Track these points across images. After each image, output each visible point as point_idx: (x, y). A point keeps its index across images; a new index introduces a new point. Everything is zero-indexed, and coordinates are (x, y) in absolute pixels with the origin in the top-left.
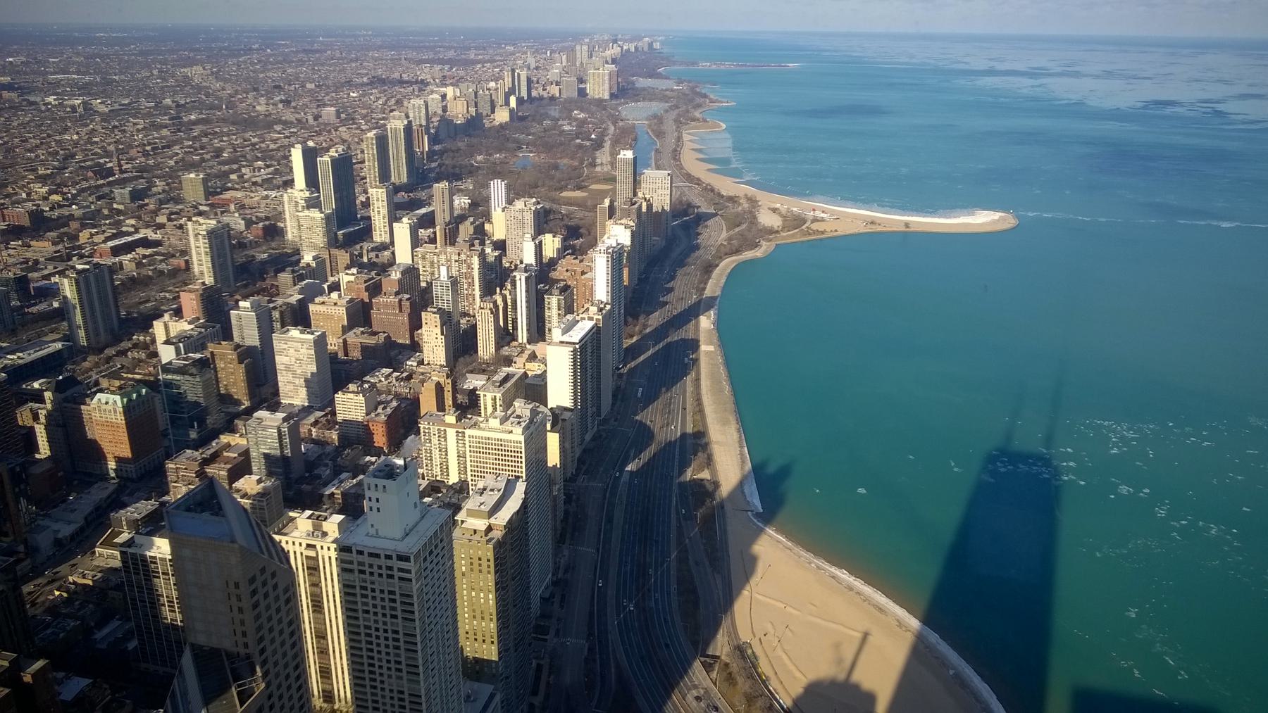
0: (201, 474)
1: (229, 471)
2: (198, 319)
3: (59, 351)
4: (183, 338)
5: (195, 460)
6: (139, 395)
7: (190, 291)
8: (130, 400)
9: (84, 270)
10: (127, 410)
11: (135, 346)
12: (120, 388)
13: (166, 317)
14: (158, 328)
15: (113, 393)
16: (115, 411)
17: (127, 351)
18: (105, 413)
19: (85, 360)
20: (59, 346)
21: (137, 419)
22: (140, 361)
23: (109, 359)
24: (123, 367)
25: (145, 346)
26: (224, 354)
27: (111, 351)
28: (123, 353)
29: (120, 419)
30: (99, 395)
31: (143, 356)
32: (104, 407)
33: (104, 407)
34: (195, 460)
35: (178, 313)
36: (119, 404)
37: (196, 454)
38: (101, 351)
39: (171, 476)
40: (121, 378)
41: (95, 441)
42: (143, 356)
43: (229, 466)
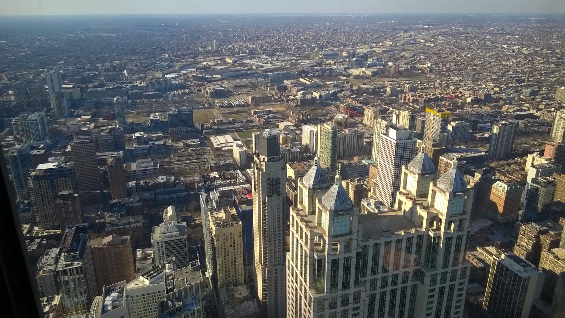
0: (537, 237)
1: (551, 241)
2: (551, 159)
3: (483, 156)
4: (541, 167)
5: (536, 229)
6: (516, 188)
7: (551, 145)
8: (511, 189)
9: (505, 124)
10: (508, 192)
11: (516, 163)
12: (509, 182)
13: (535, 154)
14: (530, 158)
15: (505, 183)
16: (503, 191)
17: (511, 164)
18: (499, 190)
19: (492, 162)
20: (483, 153)
21: (512, 197)
22: (516, 170)
23: (502, 166)
24: (507, 171)
25: (520, 164)
26: (560, 181)
27: (504, 162)
28: (509, 165)
29: (504, 195)
30: (498, 182)
31: (518, 169)
32: (499, 188)
33: (499, 188)
34: (536, 229)
35: (541, 154)
36: (506, 189)
37: (538, 227)
38: (500, 160)
39: (521, 232)
40: (505, 176)
41: (495, 203)
42: (518, 169)
43: (552, 239)
